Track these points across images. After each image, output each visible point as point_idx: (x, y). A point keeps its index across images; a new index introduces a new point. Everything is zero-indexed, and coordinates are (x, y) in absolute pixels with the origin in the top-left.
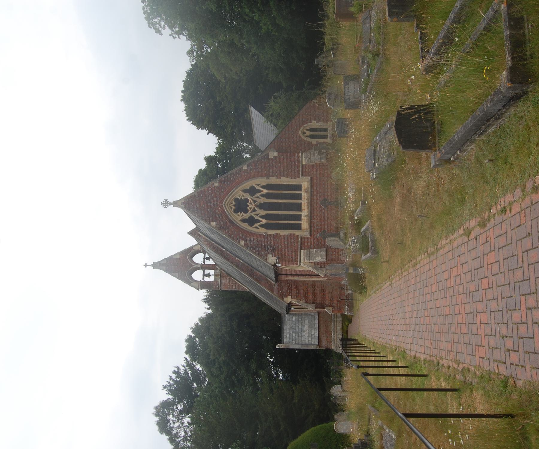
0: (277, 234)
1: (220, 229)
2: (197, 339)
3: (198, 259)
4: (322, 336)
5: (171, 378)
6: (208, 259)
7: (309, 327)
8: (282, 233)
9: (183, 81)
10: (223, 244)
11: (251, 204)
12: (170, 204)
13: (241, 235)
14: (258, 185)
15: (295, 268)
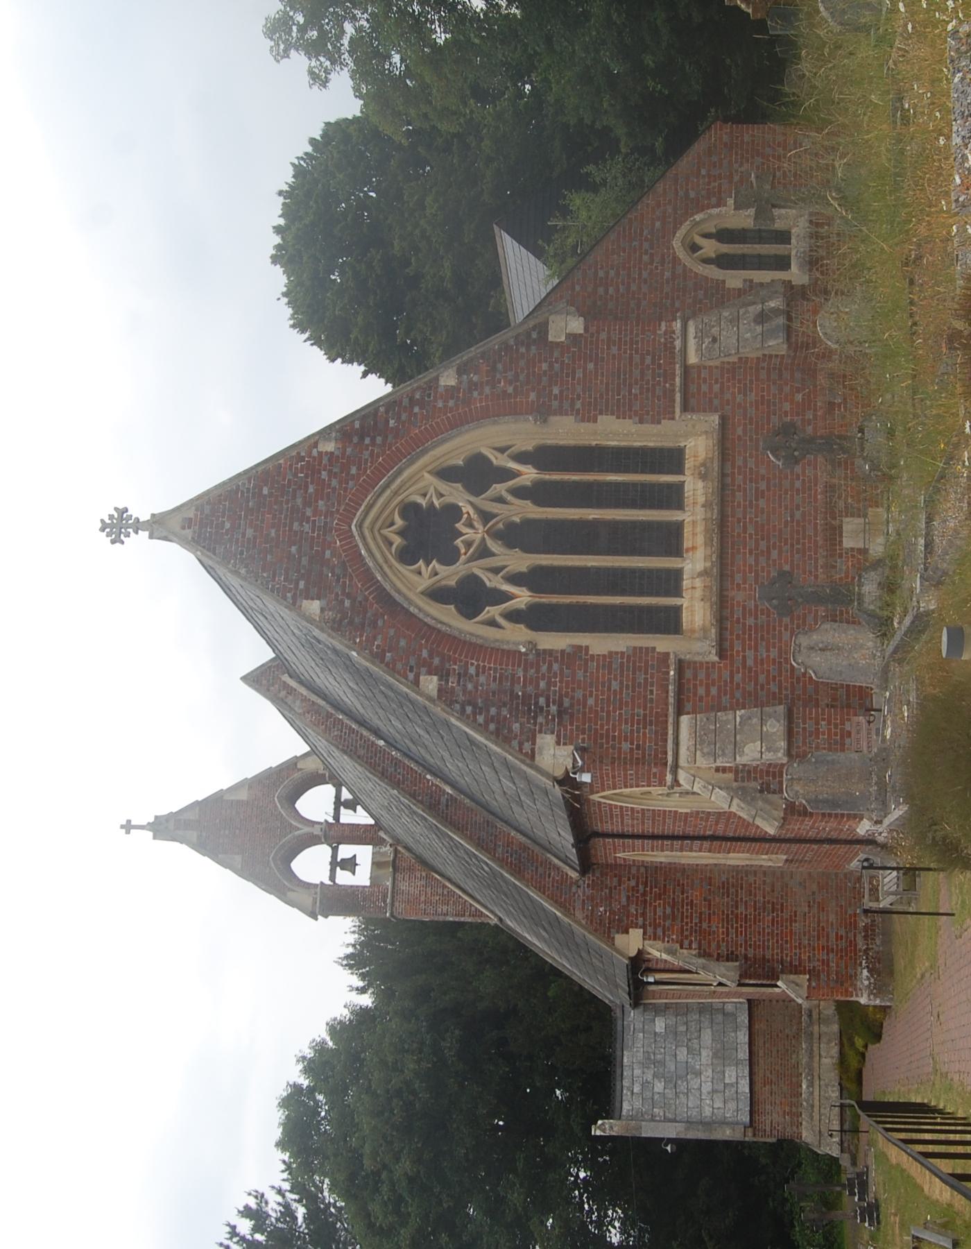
0: (579, 648)
1: (336, 626)
2: (320, 1097)
3: (317, 804)
4: (763, 1092)
5: (233, 1232)
6: (351, 805)
7: (715, 1055)
8: (600, 644)
9: (280, 193)
10: (376, 722)
11: (470, 525)
12: (138, 526)
13: (425, 654)
14: (502, 450)
15: (659, 799)
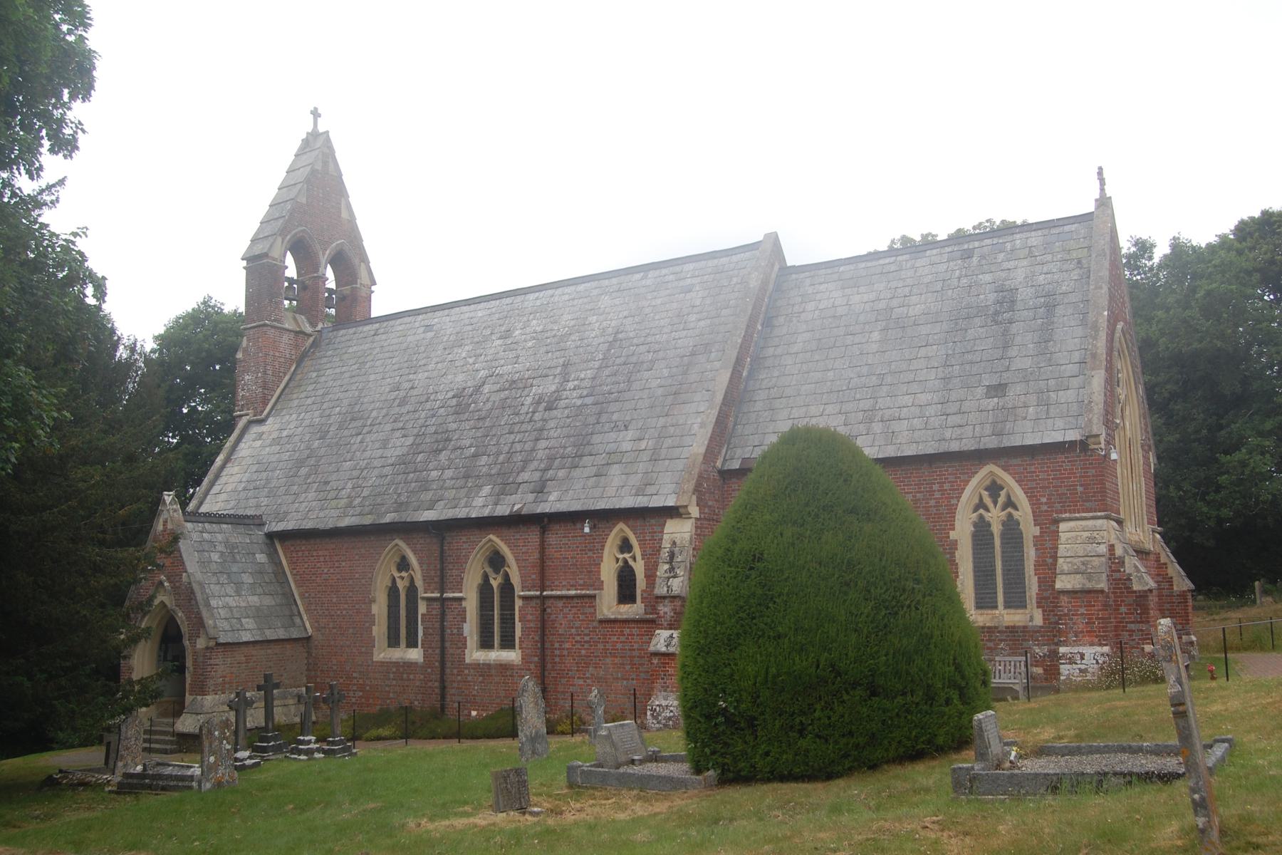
7: (258, 609)
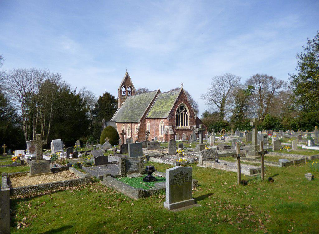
8: (176, 120)
